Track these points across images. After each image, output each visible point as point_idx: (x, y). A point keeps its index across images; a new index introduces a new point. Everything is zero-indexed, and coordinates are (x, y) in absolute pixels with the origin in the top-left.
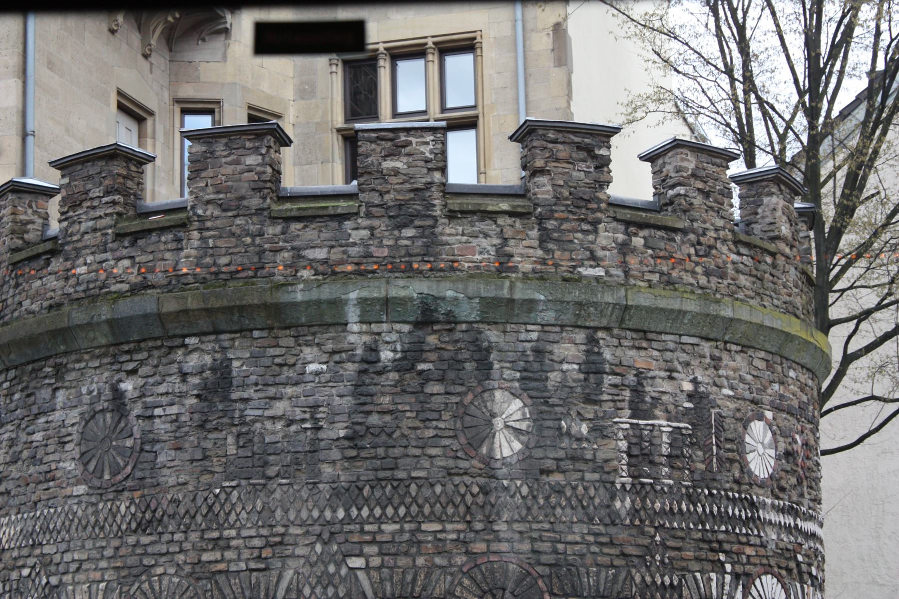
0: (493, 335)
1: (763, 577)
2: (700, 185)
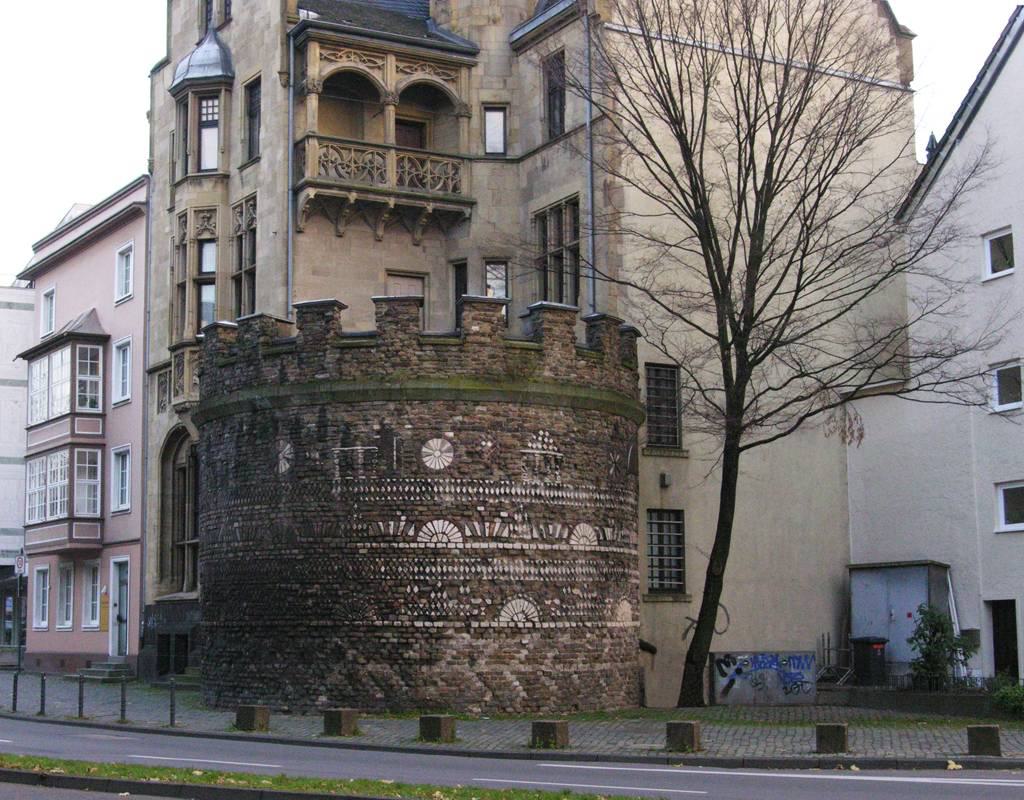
0: (278, 414)
1: (435, 522)
2: (389, 319)
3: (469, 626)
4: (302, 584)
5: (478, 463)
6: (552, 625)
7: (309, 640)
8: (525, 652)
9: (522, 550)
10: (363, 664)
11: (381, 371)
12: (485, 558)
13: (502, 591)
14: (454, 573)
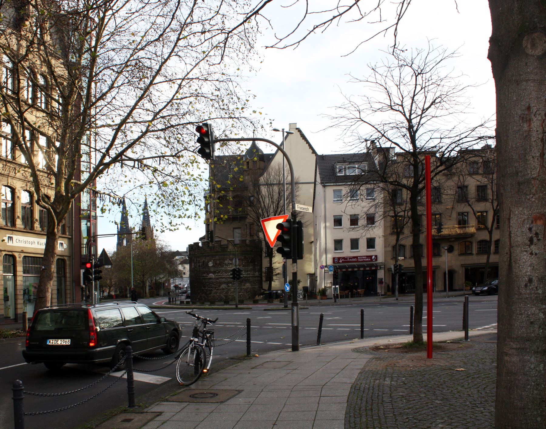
12: (218, 279)
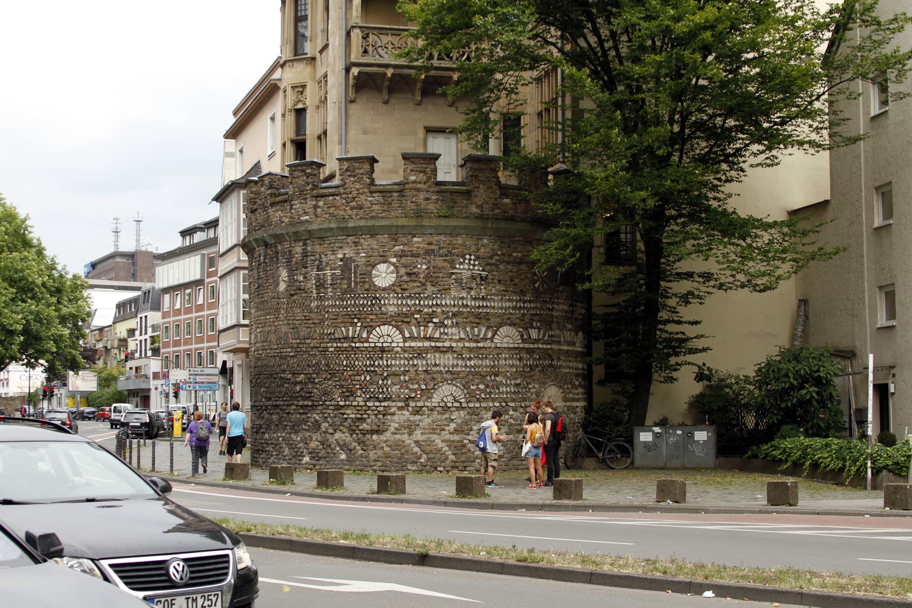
1: (382, 327)
2: (348, 173)
3: (408, 405)
4: (293, 374)
5: (415, 281)
6: (477, 405)
7: (298, 416)
8: (453, 426)
9: (451, 347)
10: (332, 434)
11: (343, 213)
12: (420, 353)
13: (434, 379)
14: (396, 365)
